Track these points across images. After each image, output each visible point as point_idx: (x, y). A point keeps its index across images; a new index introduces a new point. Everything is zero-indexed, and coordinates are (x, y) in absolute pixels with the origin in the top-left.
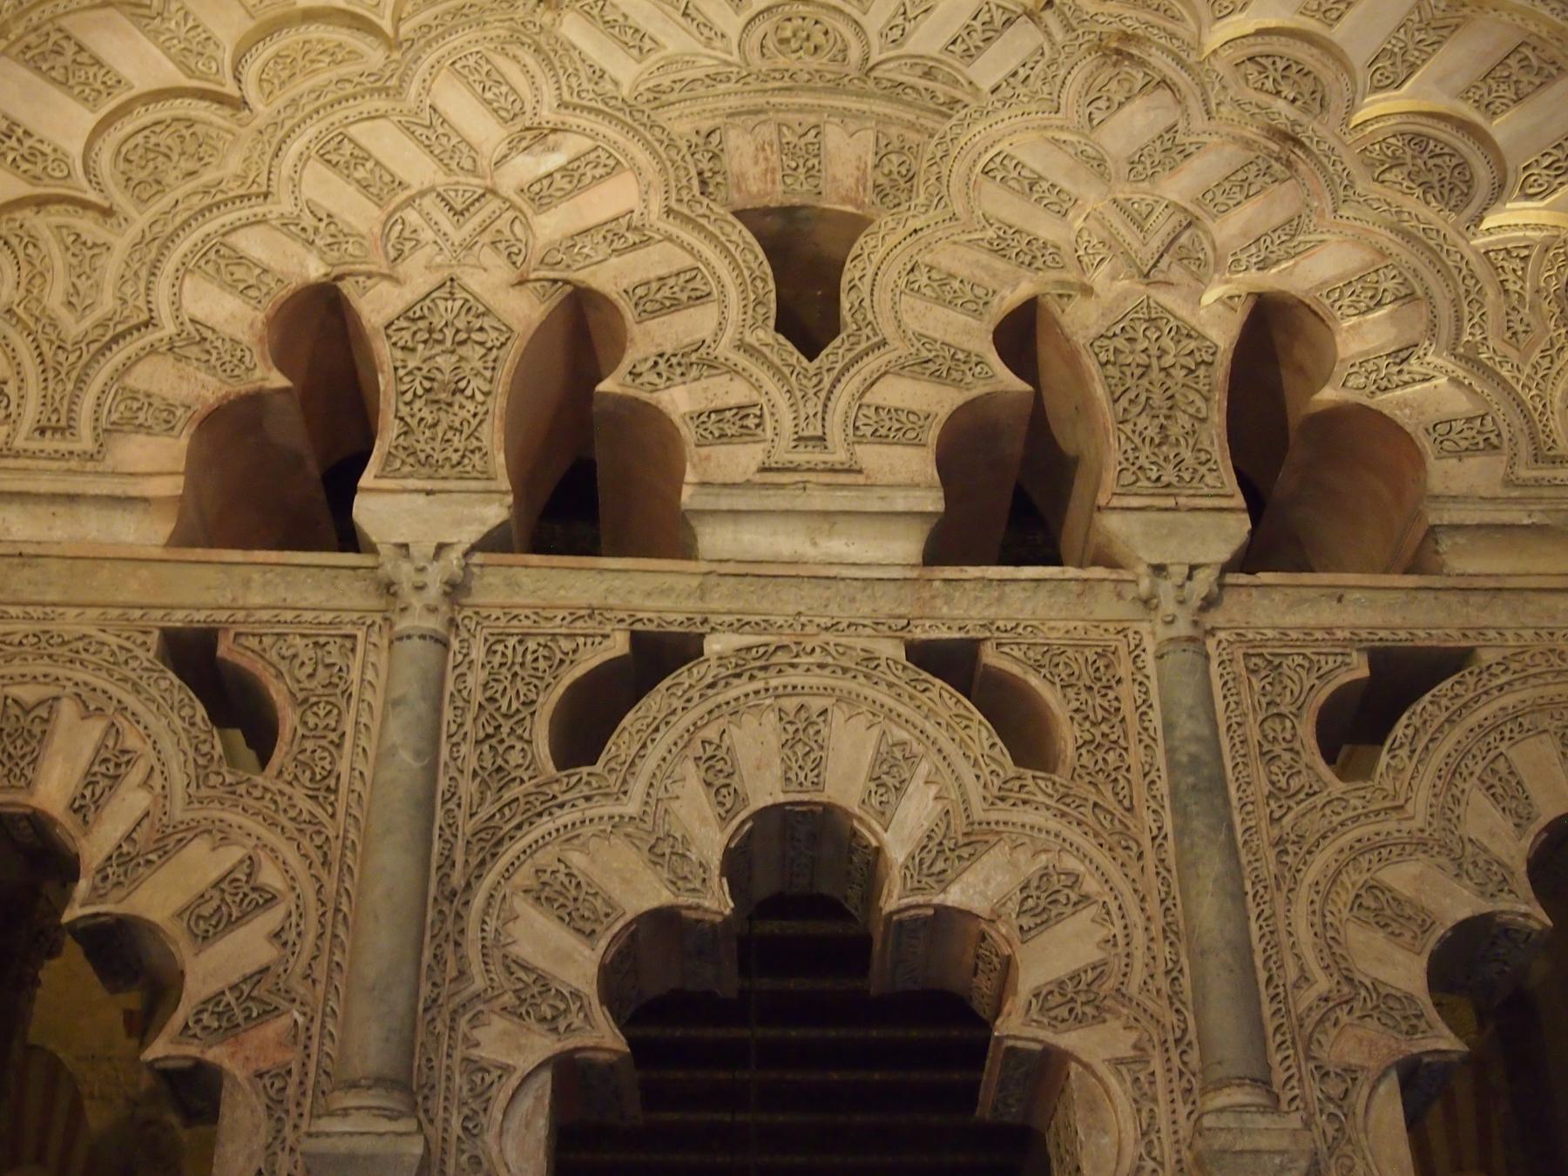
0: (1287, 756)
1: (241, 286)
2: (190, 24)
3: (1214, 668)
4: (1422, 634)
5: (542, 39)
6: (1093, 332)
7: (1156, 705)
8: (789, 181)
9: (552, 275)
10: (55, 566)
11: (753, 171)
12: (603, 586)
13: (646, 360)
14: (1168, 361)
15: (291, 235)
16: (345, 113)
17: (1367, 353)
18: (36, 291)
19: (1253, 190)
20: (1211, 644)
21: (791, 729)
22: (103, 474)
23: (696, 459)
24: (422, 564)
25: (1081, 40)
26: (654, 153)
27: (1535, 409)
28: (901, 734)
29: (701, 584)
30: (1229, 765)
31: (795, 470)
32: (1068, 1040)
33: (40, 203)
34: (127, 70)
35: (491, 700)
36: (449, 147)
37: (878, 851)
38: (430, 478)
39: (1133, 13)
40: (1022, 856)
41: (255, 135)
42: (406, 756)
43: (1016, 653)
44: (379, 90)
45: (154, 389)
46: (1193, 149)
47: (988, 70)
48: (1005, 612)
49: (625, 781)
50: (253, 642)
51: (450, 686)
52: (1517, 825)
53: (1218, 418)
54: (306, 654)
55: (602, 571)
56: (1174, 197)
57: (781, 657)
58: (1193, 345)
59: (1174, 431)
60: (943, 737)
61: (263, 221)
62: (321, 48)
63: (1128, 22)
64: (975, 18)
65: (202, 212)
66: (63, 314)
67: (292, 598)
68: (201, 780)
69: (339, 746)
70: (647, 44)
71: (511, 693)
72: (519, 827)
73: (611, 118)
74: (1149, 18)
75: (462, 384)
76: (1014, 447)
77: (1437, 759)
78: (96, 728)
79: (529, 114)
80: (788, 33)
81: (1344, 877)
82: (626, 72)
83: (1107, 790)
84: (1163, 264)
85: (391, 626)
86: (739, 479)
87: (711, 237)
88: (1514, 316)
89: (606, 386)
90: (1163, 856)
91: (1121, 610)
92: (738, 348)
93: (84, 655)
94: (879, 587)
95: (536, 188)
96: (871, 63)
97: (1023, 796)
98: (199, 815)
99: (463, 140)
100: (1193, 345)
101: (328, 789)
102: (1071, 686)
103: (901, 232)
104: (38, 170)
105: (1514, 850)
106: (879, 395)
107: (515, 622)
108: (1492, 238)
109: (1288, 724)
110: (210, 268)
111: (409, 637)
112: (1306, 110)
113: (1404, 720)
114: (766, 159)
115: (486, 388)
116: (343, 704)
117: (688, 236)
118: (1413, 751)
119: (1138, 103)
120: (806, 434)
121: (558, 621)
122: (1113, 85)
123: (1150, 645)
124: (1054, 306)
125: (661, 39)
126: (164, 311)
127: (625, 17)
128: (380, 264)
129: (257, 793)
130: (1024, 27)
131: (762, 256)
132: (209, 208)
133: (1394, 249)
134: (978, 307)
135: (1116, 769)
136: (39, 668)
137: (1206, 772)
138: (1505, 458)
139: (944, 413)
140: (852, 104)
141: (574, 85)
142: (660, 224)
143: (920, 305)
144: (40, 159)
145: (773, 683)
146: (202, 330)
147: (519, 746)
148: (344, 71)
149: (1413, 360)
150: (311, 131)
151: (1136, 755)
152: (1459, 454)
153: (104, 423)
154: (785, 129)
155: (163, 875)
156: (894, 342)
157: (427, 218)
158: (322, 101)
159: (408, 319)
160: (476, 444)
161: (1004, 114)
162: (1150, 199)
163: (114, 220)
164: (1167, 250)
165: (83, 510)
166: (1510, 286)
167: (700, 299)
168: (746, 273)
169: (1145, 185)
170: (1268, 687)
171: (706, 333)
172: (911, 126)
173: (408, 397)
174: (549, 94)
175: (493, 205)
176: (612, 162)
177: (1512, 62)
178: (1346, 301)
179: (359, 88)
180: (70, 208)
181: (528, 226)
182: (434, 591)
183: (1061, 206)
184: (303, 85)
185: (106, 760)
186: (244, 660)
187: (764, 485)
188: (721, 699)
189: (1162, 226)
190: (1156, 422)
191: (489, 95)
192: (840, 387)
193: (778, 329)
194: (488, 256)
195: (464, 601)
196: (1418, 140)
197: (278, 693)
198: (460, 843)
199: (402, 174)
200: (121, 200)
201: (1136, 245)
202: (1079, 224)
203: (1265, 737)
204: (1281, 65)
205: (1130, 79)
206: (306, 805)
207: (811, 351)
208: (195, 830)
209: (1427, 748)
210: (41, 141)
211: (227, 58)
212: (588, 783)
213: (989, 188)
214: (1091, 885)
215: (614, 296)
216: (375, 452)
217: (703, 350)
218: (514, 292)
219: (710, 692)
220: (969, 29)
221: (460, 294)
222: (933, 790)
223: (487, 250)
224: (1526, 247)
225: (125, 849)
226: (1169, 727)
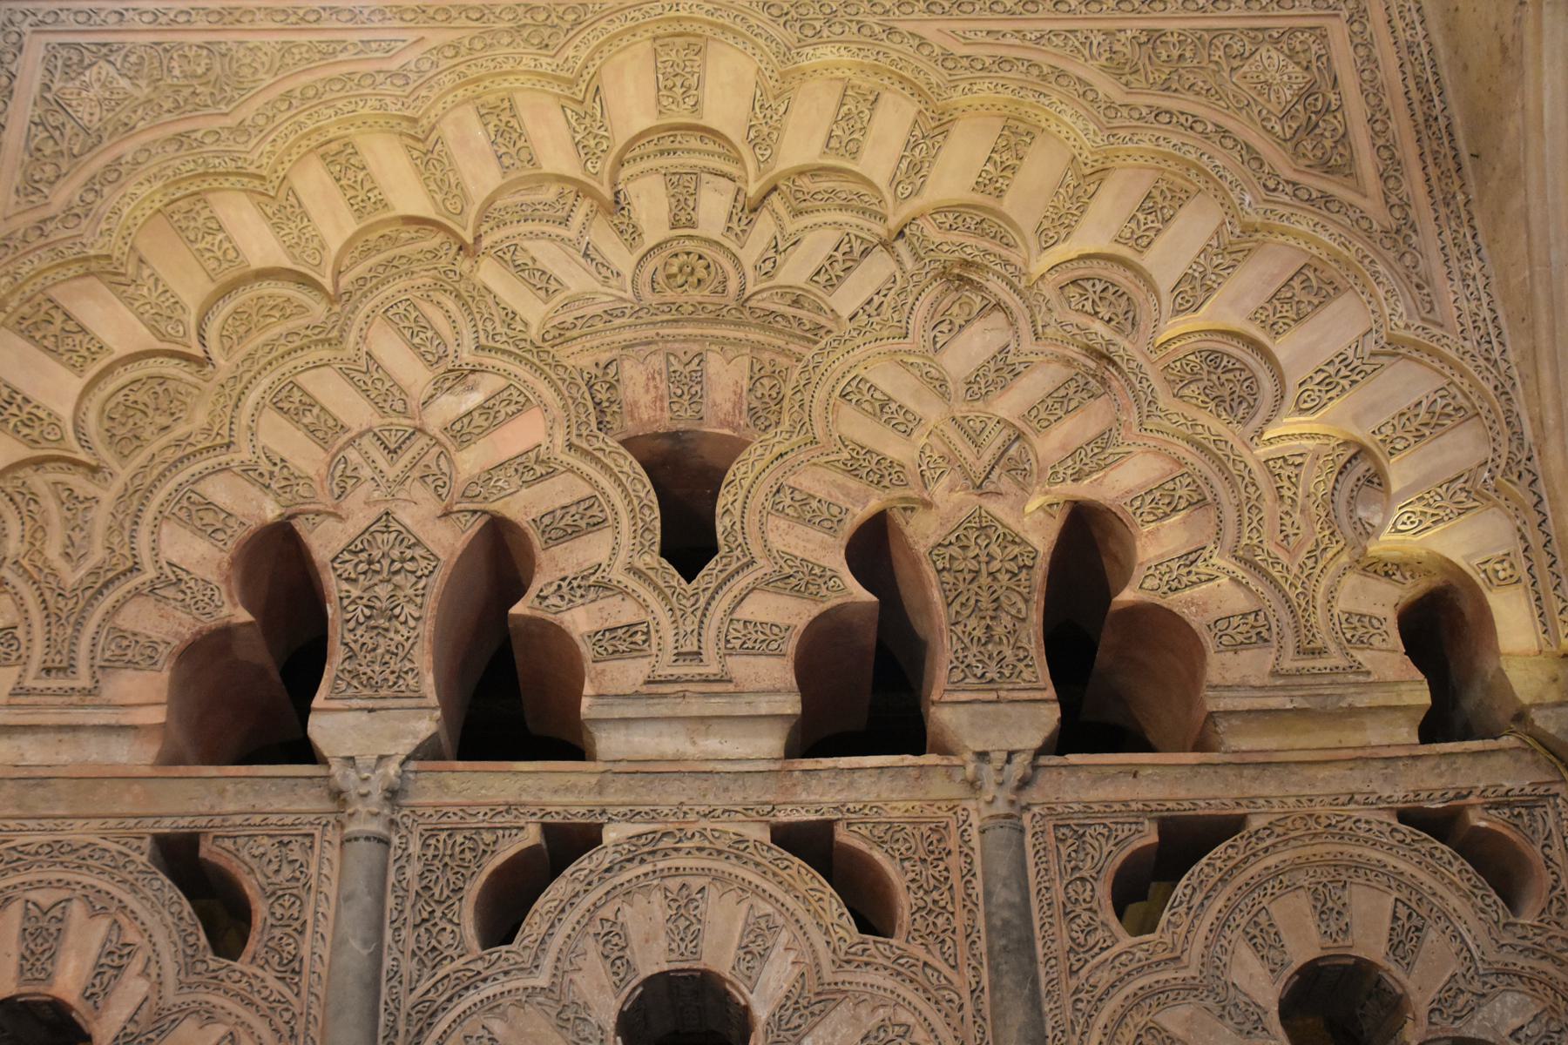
0: (1085, 916)
1: (210, 530)
2: (160, 289)
3: (1028, 840)
4: (1203, 804)
5: (462, 287)
6: (932, 541)
7: (979, 875)
8: (675, 407)
9: (472, 506)
10: (62, 785)
11: (645, 399)
12: (517, 785)
13: (551, 584)
14: (996, 565)
15: (253, 482)
16: (293, 363)
17: (1162, 556)
18: (38, 544)
19: (1073, 405)
20: (1027, 817)
21: (674, 905)
22: (100, 706)
23: (593, 674)
24: (366, 775)
25: (927, 269)
26: (557, 390)
27: (1300, 606)
28: (768, 909)
29: (599, 781)
30: (1037, 924)
31: (675, 682)
33: (38, 463)
34: (108, 336)
35: (427, 888)
36: (384, 390)
37: (746, 1009)
38: (371, 698)
39: (972, 241)
40: (863, 1011)
41: (218, 389)
42: (355, 944)
43: (863, 831)
44: (322, 341)
45: (137, 630)
46: (1021, 368)
47: (847, 299)
48: (854, 795)
49: (536, 957)
50: (228, 843)
51: (392, 878)
52: (1272, 971)
53: (1036, 617)
54: (273, 852)
55: (516, 773)
56: (1003, 414)
57: (667, 843)
58: (1017, 550)
59: (999, 630)
60: (798, 908)
61: (226, 468)
62: (272, 303)
63: (969, 250)
64: (836, 250)
65: (175, 465)
67: (261, 805)
68: (189, 964)
69: (301, 933)
70: (553, 286)
71: (442, 882)
72: (450, 1000)
73: (521, 359)
74: (985, 244)
75: (397, 611)
76: (870, 639)
77: (1209, 917)
78: (103, 924)
79: (451, 358)
80: (675, 270)
81: (1128, 1019)
83: (936, 949)
84: (994, 476)
85: (343, 827)
86: (628, 692)
87: (605, 467)
88: (1287, 520)
89: (518, 609)
90: (980, 1006)
91: (955, 790)
92: (629, 570)
93: (90, 862)
94: (748, 780)
95: (458, 426)
96: (747, 293)
97: (865, 958)
98: (189, 999)
99: (395, 384)
100: (1017, 550)
101: (293, 971)
102: (908, 859)
103: (768, 457)
104: (35, 434)
105: (1267, 993)
106: (748, 610)
107: (445, 819)
108: (1272, 447)
109: (1089, 887)
110: (183, 514)
111: (356, 839)
112: (1119, 330)
113: (1184, 881)
114: (656, 387)
115: (416, 615)
116: (303, 894)
117: (588, 468)
118: (1190, 909)
119: (978, 325)
120: (684, 650)
121: (480, 817)
122: (955, 309)
123: (975, 820)
124: (898, 517)
125: (565, 280)
126: (145, 557)
127: (534, 260)
128: (326, 502)
129: (236, 976)
130: (879, 255)
131: (649, 486)
132: (181, 460)
133: (1190, 459)
135: (944, 931)
136: (54, 874)
137: (1015, 935)
138: (1274, 650)
139: (801, 624)
140: (732, 333)
141: (489, 329)
142: (563, 457)
143: (783, 524)
144: (37, 423)
145: (660, 865)
146: (179, 572)
147: (449, 927)
148: (291, 324)
149: (1199, 563)
150: (265, 382)
151: (960, 921)
152: (1236, 648)
153: (98, 662)
154: (672, 358)
156: (761, 562)
157: (366, 456)
158: (274, 354)
159: (351, 552)
160: (409, 665)
161: (859, 341)
162: (983, 416)
163: (99, 476)
164: (997, 463)
165: (83, 736)
166: (1285, 492)
167: (597, 525)
168: (636, 502)
169: (979, 405)
170: (1073, 855)
172: (782, 352)
173: (352, 624)
175: (421, 442)
176: (521, 399)
177: (1296, 283)
178: (1146, 509)
179: (305, 340)
180: (64, 465)
181: (450, 461)
182: (377, 796)
183: (904, 424)
184: (258, 340)
185: (111, 953)
186: (222, 862)
187: (650, 696)
188: (617, 881)
190: (983, 623)
191: (417, 340)
192: (714, 603)
193: (664, 553)
194: (419, 491)
195: (403, 802)
196: (1213, 357)
197: (250, 887)
198: (402, 1016)
199: (344, 419)
200: (107, 456)
201: (971, 459)
202: (923, 440)
203: (1069, 898)
204: (1099, 287)
206: (279, 986)
207: (689, 574)
208: (186, 1011)
209: (1202, 904)
210: (38, 407)
211: (192, 320)
212: (507, 959)
213: (847, 410)
215: (525, 525)
216: (325, 676)
217: (598, 574)
218: (440, 524)
219: (607, 875)
220: (831, 260)
221: (394, 526)
222: (792, 956)
223: (417, 484)
224: (1301, 455)
225: (131, 1028)
226: (988, 894)
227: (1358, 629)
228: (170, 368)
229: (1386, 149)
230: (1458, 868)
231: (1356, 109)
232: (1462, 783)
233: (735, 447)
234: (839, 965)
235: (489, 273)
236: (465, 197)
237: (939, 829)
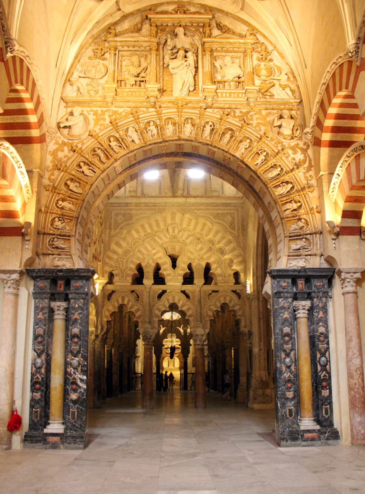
32: (190, 318)
34: (123, 245)
37: (178, 306)
47: (188, 241)
89: (160, 272)
124: (192, 263)
167: (166, 264)
171: (167, 267)
184: (136, 245)
189: (201, 256)
196: (220, 249)
207: (174, 269)
213: (188, 253)
227: (229, 276)
228: (129, 248)
229: (238, 227)
231: (236, 222)
235: (156, 238)
237: (194, 291)
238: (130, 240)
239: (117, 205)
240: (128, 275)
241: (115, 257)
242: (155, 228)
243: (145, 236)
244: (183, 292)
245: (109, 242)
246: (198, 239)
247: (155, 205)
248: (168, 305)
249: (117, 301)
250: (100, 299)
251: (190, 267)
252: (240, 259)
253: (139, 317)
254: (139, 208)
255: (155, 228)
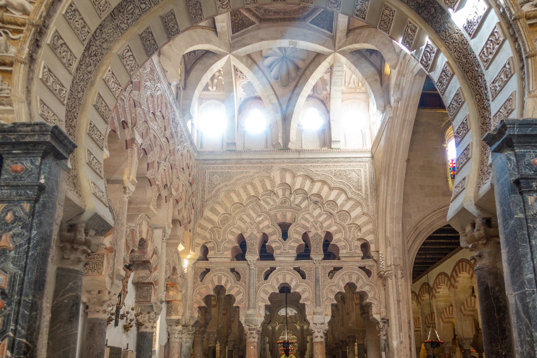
34: (220, 212)
47: (303, 206)
66: (218, 239)
68: (235, 282)
78: (226, 278)
82: (268, 208)
89: (267, 244)
112: (333, 210)
117: (274, 227)
128: (245, 231)
134: (300, 234)
155: (233, 290)
174: (260, 211)
175: (255, 223)
184: (237, 211)
194: (255, 229)
205: (317, 206)
214: (308, 290)
228: (227, 215)
230: (364, 273)
232: (365, 264)
233: (290, 224)
234: (300, 282)
235: (262, 202)
236: (259, 193)
238: (229, 205)
239: (213, 162)
240: (226, 249)
241: (210, 226)
242: (261, 190)
243: (247, 199)
244: (298, 270)
245: (202, 207)
246: (316, 203)
247: (260, 161)
248: (277, 287)
249: (212, 281)
250: (190, 280)
251: (305, 237)
252: (370, 227)
253: (241, 301)
254: (240, 165)
255: (261, 190)
